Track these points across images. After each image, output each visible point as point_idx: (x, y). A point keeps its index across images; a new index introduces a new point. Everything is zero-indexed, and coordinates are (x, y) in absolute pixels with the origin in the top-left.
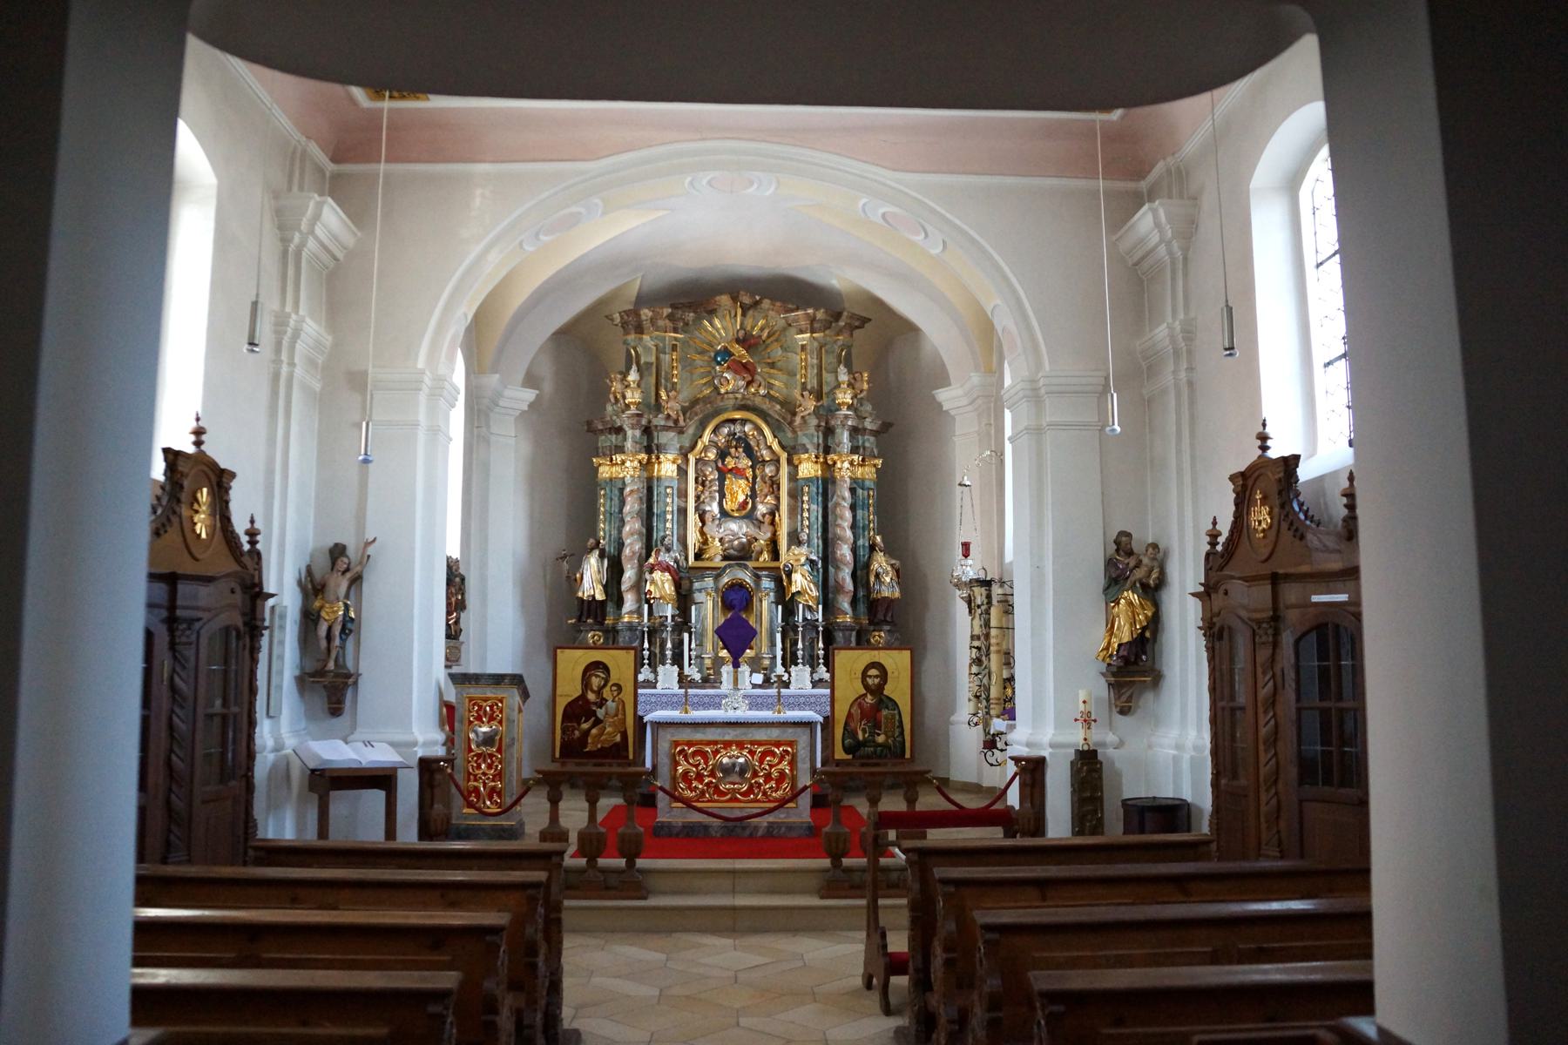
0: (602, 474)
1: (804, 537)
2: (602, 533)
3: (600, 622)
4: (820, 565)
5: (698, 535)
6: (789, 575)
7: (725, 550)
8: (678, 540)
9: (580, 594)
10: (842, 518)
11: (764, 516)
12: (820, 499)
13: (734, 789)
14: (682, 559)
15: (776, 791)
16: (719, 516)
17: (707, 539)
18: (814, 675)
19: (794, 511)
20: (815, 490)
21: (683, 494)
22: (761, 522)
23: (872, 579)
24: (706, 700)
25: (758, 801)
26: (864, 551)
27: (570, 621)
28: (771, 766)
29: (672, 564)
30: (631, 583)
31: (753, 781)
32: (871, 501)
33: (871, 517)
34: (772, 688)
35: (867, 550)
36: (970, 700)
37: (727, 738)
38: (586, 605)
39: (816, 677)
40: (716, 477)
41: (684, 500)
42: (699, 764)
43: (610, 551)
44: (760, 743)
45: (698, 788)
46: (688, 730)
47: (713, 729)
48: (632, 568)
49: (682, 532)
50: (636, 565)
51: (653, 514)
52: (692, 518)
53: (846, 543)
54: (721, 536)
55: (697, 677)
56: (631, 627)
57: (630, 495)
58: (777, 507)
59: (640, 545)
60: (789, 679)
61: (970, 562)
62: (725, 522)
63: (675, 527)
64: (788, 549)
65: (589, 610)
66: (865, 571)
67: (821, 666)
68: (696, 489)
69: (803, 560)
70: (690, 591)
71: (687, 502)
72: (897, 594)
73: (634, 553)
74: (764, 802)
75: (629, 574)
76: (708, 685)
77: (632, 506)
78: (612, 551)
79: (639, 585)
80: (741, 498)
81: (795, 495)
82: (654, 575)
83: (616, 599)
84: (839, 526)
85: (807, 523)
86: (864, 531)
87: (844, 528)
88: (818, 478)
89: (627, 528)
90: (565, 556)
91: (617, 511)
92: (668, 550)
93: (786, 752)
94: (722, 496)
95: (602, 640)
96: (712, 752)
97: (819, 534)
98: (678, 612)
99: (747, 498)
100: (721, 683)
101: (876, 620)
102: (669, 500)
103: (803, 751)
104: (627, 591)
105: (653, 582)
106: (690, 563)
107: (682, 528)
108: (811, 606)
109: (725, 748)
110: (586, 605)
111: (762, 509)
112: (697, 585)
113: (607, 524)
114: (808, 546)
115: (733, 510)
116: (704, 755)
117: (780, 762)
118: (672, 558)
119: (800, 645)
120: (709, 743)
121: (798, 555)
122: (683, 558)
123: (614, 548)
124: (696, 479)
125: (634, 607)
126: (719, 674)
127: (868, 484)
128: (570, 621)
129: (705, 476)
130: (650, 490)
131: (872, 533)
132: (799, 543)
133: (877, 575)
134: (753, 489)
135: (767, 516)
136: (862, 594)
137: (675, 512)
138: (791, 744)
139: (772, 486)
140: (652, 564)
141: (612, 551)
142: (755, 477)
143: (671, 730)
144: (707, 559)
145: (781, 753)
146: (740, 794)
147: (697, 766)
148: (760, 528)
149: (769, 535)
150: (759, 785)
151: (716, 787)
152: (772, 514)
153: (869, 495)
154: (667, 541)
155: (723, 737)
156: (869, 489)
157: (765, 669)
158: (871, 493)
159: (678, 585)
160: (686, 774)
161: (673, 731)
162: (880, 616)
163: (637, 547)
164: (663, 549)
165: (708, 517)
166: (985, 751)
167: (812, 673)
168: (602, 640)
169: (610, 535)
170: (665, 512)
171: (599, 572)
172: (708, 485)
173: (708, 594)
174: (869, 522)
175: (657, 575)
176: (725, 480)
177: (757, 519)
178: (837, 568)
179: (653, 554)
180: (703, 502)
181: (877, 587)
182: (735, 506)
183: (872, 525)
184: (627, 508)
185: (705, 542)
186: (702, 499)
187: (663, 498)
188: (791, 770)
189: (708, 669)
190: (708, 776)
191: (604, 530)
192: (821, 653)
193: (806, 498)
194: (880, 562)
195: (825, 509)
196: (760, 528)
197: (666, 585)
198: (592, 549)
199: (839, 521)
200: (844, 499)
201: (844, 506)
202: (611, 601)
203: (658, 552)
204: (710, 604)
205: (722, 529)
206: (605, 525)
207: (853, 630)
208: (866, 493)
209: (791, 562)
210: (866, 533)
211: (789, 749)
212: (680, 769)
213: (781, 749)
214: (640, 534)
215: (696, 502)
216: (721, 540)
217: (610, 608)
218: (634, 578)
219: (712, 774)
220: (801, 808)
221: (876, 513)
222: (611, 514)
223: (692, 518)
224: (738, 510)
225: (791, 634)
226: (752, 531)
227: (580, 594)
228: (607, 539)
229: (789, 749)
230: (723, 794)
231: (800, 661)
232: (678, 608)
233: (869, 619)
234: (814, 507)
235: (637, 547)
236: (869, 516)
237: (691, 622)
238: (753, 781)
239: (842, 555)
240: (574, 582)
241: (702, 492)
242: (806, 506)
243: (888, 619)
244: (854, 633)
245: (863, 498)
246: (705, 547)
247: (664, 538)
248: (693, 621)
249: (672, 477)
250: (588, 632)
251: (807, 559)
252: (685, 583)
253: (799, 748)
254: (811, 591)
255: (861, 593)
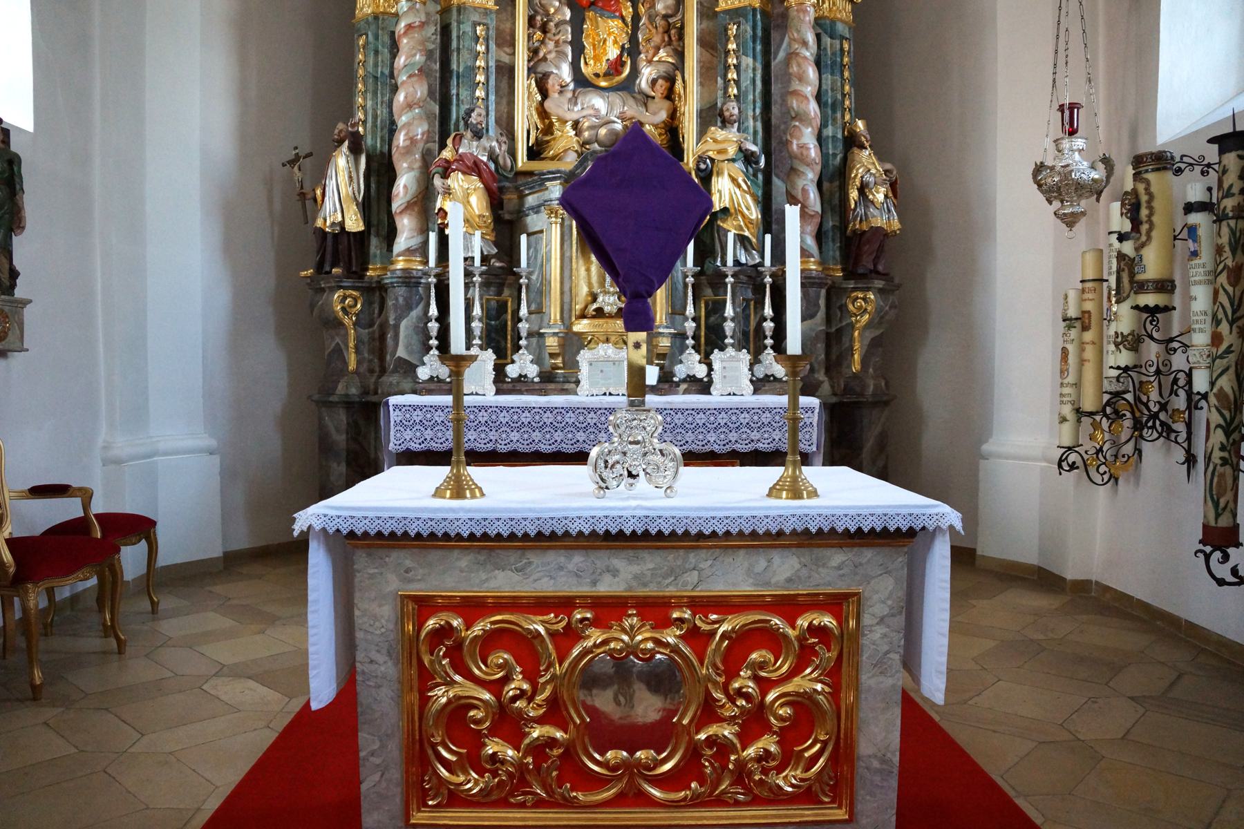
0: (362, 9)
1: (733, 109)
2: (360, 115)
3: (356, 271)
4: (762, 163)
5: (536, 117)
6: (707, 177)
7: (583, 145)
8: (497, 122)
9: (319, 223)
10: (802, 78)
11: (654, 82)
12: (759, 48)
13: (631, 769)
14: (501, 150)
15: (780, 769)
16: (572, 86)
17: (551, 125)
18: (756, 368)
19: (713, 69)
20: (749, 29)
21: (508, 41)
22: (648, 96)
23: (854, 195)
24: (548, 418)
25: (720, 802)
26: (835, 148)
27: (303, 273)
28: (765, 685)
29: (485, 159)
30: (408, 198)
31: (702, 736)
32: (846, 60)
33: (847, 88)
34: (676, 393)
35: (840, 146)
36: (1063, 420)
37: (607, 587)
38: (329, 239)
39: (760, 371)
40: (568, 18)
41: (507, 50)
42: (507, 679)
43: (374, 147)
44: (725, 605)
45: (503, 762)
46: (464, 560)
47: (553, 558)
48: (410, 169)
49: (504, 108)
50: (417, 165)
51: (451, 72)
52: (523, 83)
53: (810, 124)
54: (575, 116)
55: (532, 371)
56: (410, 280)
57: (405, 33)
58: (680, 65)
59: (425, 127)
60: (709, 375)
61: (1079, 143)
62: (585, 93)
63: (492, 98)
64: (702, 133)
65: (336, 252)
66: (837, 183)
67: (769, 351)
68: (530, 37)
69: (732, 151)
70: (520, 213)
71: (514, 54)
72: (896, 225)
73: (413, 141)
74: (737, 803)
75: (405, 184)
76: (552, 386)
77: (409, 56)
78: (378, 145)
79: (424, 202)
80: (613, 53)
81: (712, 43)
82: (449, 181)
83: (384, 232)
84: (795, 93)
85: (735, 91)
86: (834, 111)
87: (806, 98)
88: (754, 10)
89: (401, 97)
90: (297, 157)
91: (387, 72)
92: (478, 135)
93: (819, 631)
94: (578, 49)
95: (359, 306)
96: (553, 635)
97: (758, 111)
98: (495, 251)
99: (621, 56)
100: (578, 382)
101: (861, 271)
102: (481, 48)
103: (880, 631)
104: (401, 213)
105: (448, 192)
106: (520, 164)
107: (504, 101)
108: (747, 238)
109: (596, 623)
110: (329, 239)
111: (647, 73)
112: (531, 200)
113: (369, 96)
114: (739, 130)
115: (597, 75)
116: (525, 646)
117: (794, 672)
118: (485, 149)
119: (729, 311)
120: (540, 605)
121: (724, 141)
122: (504, 147)
123: (382, 138)
124: (531, 22)
125: (415, 242)
126: (573, 365)
127: (841, 28)
128: (303, 273)
129: (547, 14)
130: (445, 31)
131: (847, 117)
132: (725, 123)
133: (863, 189)
134: (633, 39)
135: (660, 82)
136: (831, 224)
137: (493, 70)
138: (835, 603)
139: (667, 31)
140: (447, 161)
141: (378, 145)
142: (636, 17)
143: (405, 558)
144: (552, 158)
145: (801, 639)
146: (659, 782)
147: (497, 687)
148: (645, 105)
149: (663, 116)
150: (722, 748)
151: (570, 756)
152: (671, 80)
153: (842, 49)
154: (474, 119)
155: (594, 583)
156: (842, 38)
157: (662, 356)
158: (846, 46)
159: (495, 200)
160: (459, 708)
161: (408, 563)
162: (867, 263)
163: (420, 131)
164: (469, 134)
165: (552, 84)
166: (1208, 549)
167: (752, 365)
168: (359, 306)
169: (375, 117)
170: (473, 70)
171: (350, 177)
172: (553, 30)
173: (552, 212)
174: (844, 95)
175: (457, 181)
176: (583, 21)
177: (641, 92)
178: (793, 172)
179: (449, 142)
180: (545, 59)
181: (861, 211)
182: (603, 67)
183: (847, 103)
184: (401, 60)
185: (548, 130)
186: (541, 54)
187: (467, 43)
188: (835, 695)
189: (552, 356)
190: (541, 721)
191: (364, 107)
192: (769, 326)
193: (732, 46)
194: (866, 164)
195: (767, 67)
196: (645, 105)
197: (474, 200)
198: (341, 142)
199: (796, 85)
200: (805, 44)
201: (805, 58)
202: (378, 235)
203: (459, 139)
204: (556, 232)
205: (579, 107)
206: (365, 99)
207: (820, 285)
208: (838, 42)
209: (710, 154)
210: (839, 115)
211: (828, 620)
212: (441, 695)
213: (803, 622)
214: (429, 116)
215: (529, 61)
216: (576, 125)
217: (375, 245)
218: (413, 189)
219: (554, 713)
220: (864, 821)
221: (855, 83)
222: (376, 78)
223: (523, 83)
224: (607, 75)
225: (708, 292)
226: (633, 110)
227: (319, 223)
228: (369, 125)
229: (828, 620)
230: (597, 782)
231: (729, 341)
232: (496, 244)
233: (843, 270)
234: (748, 61)
235: (420, 130)
236: (843, 86)
237: (519, 265)
238: (702, 736)
239: (801, 147)
240: (308, 201)
241: (543, 42)
242: (732, 61)
243: (880, 268)
244: (823, 292)
245: (834, 54)
246: (548, 138)
247: (469, 113)
248: (524, 262)
249: (486, 12)
250: (333, 290)
251: (740, 149)
252: (510, 198)
253: (867, 620)
254: (748, 209)
255: (830, 224)
